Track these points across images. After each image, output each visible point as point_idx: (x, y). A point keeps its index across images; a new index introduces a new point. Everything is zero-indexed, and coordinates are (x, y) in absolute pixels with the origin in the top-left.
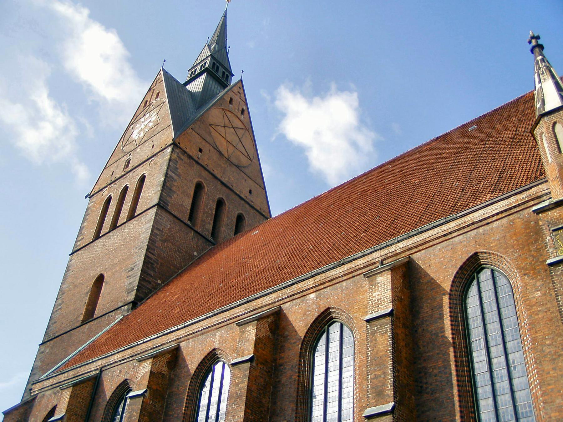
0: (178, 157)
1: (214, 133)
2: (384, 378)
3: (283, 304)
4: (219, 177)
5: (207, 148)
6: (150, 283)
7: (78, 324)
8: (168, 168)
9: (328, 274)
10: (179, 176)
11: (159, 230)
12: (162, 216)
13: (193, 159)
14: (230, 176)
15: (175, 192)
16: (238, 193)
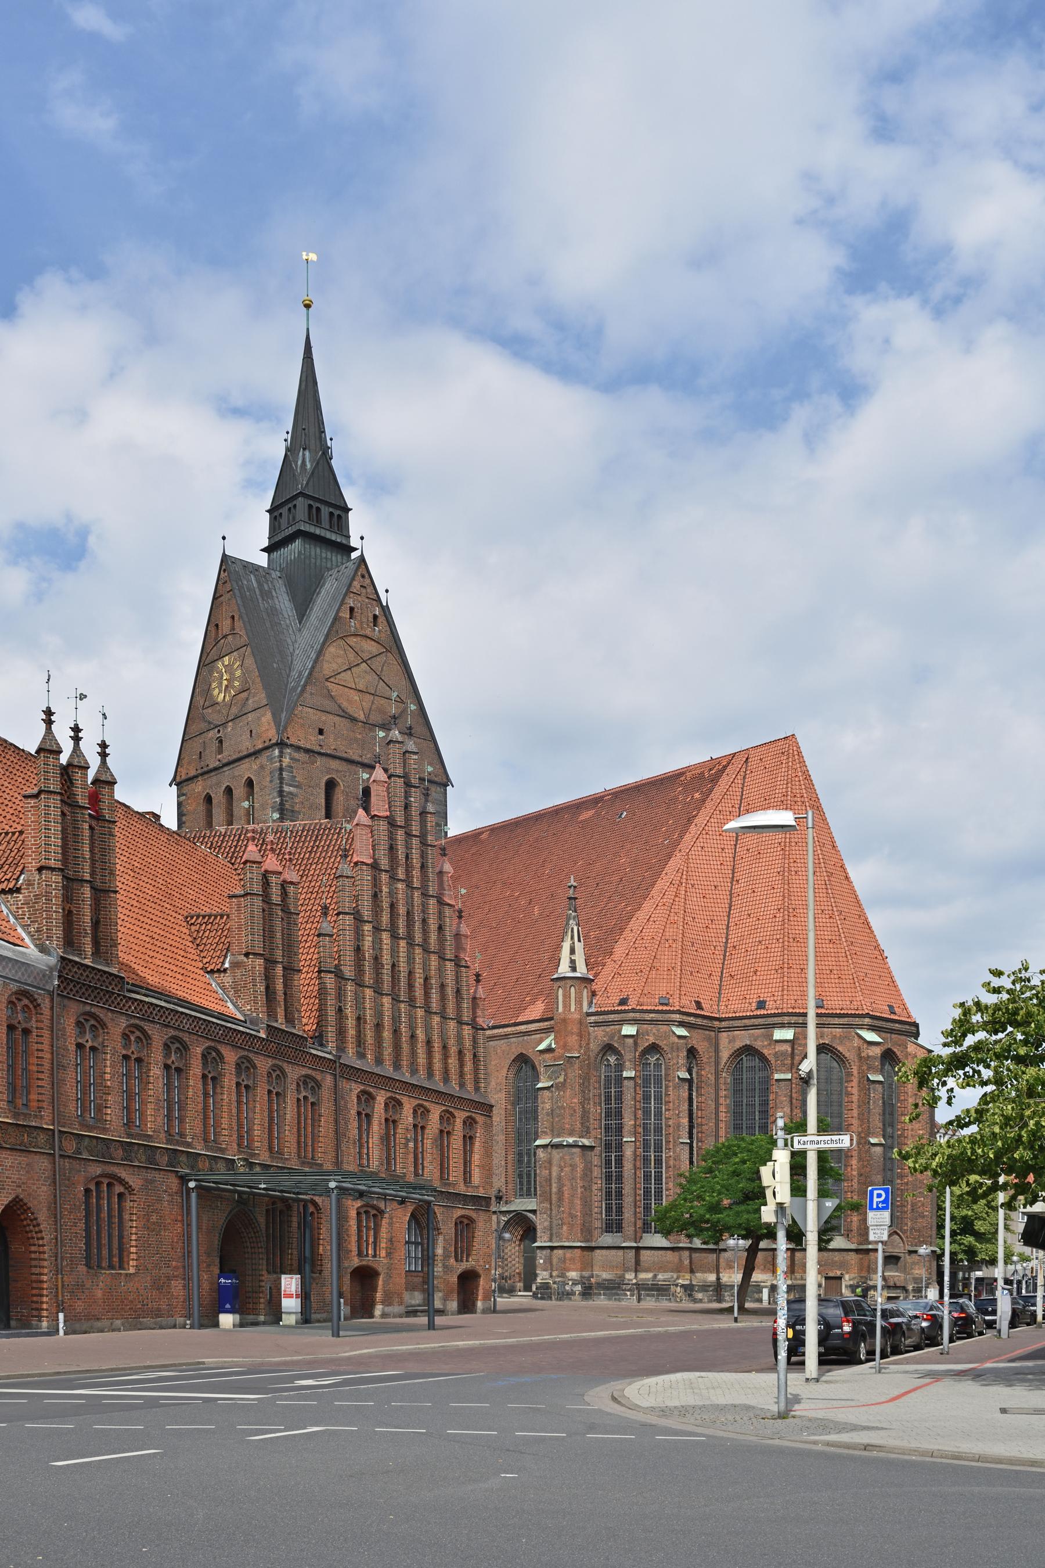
4: (356, 758)
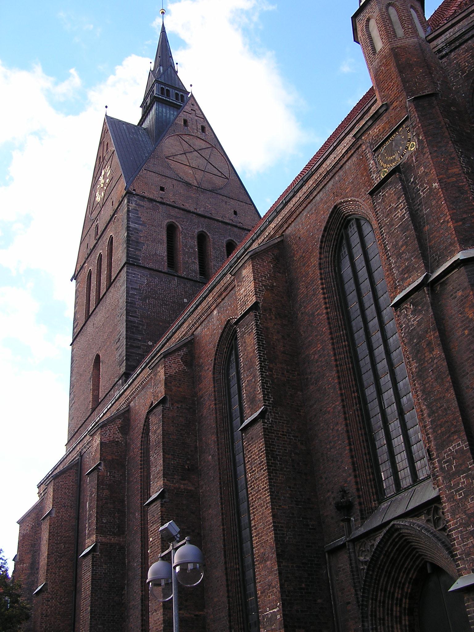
0: (137, 205)
1: (173, 165)
2: (254, 382)
3: (195, 330)
4: (192, 209)
6: (139, 347)
7: (90, 412)
8: (128, 221)
9: (222, 283)
10: (143, 224)
11: (135, 289)
12: (134, 274)
13: (156, 201)
14: (206, 204)
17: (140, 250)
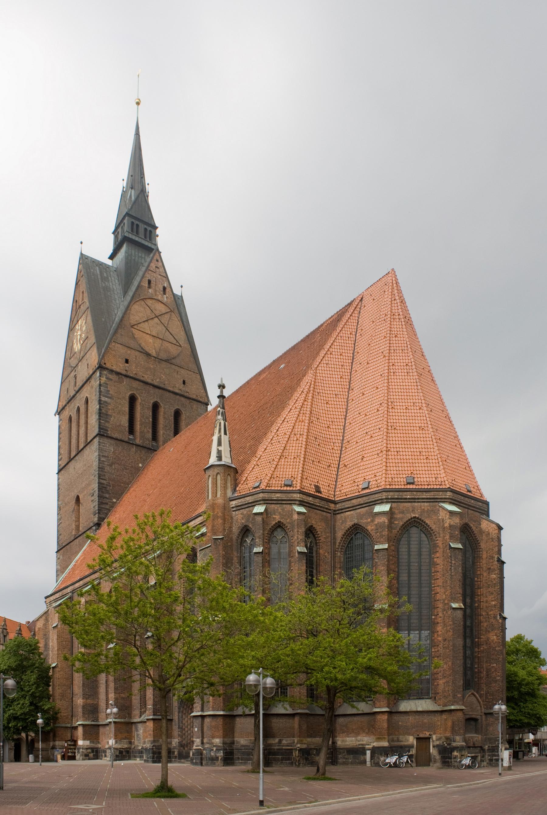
1: (137, 334)
5: (133, 355)
11: (105, 456)
12: (104, 443)
13: (121, 374)
15: (111, 416)
16: (171, 389)
17: (108, 422)
